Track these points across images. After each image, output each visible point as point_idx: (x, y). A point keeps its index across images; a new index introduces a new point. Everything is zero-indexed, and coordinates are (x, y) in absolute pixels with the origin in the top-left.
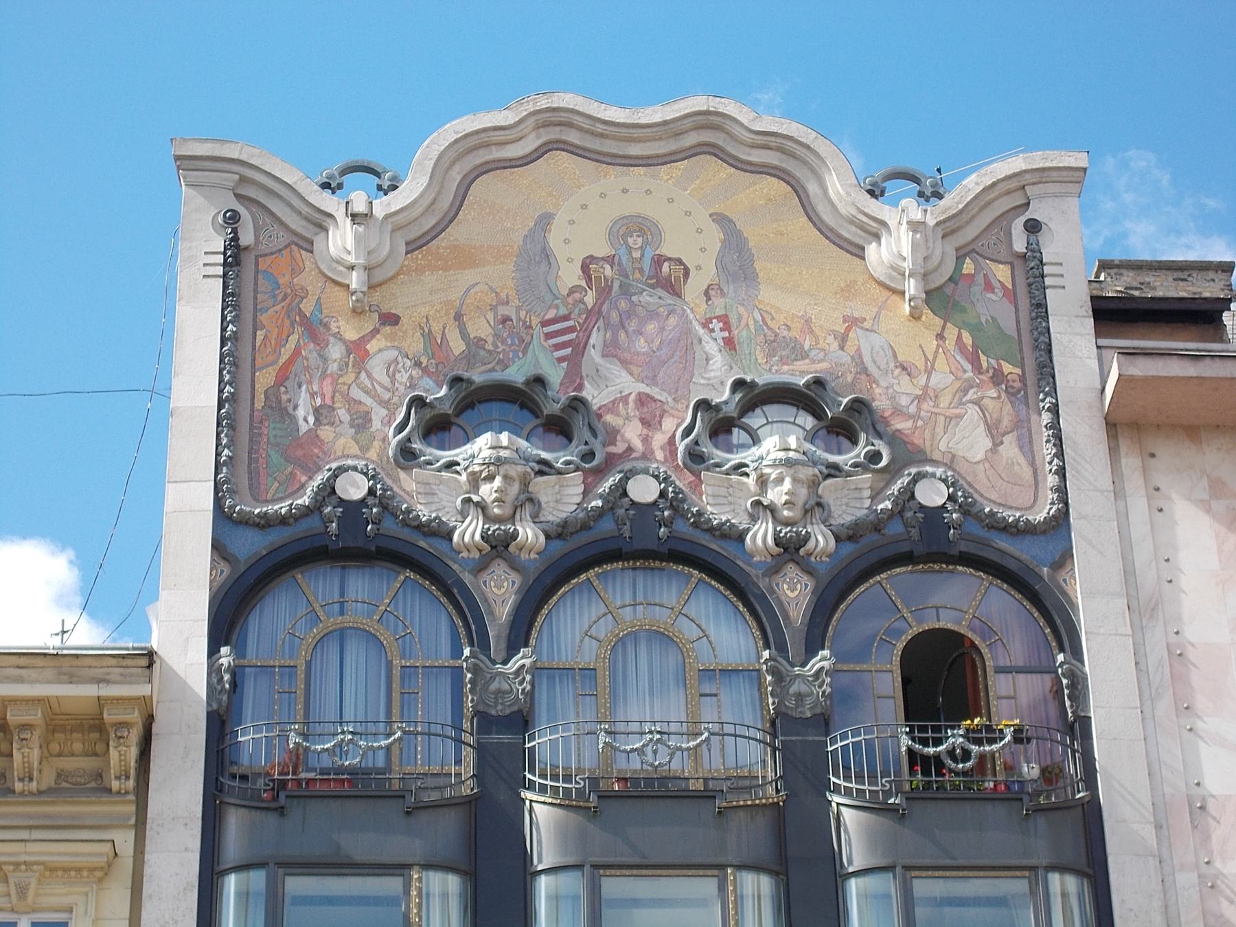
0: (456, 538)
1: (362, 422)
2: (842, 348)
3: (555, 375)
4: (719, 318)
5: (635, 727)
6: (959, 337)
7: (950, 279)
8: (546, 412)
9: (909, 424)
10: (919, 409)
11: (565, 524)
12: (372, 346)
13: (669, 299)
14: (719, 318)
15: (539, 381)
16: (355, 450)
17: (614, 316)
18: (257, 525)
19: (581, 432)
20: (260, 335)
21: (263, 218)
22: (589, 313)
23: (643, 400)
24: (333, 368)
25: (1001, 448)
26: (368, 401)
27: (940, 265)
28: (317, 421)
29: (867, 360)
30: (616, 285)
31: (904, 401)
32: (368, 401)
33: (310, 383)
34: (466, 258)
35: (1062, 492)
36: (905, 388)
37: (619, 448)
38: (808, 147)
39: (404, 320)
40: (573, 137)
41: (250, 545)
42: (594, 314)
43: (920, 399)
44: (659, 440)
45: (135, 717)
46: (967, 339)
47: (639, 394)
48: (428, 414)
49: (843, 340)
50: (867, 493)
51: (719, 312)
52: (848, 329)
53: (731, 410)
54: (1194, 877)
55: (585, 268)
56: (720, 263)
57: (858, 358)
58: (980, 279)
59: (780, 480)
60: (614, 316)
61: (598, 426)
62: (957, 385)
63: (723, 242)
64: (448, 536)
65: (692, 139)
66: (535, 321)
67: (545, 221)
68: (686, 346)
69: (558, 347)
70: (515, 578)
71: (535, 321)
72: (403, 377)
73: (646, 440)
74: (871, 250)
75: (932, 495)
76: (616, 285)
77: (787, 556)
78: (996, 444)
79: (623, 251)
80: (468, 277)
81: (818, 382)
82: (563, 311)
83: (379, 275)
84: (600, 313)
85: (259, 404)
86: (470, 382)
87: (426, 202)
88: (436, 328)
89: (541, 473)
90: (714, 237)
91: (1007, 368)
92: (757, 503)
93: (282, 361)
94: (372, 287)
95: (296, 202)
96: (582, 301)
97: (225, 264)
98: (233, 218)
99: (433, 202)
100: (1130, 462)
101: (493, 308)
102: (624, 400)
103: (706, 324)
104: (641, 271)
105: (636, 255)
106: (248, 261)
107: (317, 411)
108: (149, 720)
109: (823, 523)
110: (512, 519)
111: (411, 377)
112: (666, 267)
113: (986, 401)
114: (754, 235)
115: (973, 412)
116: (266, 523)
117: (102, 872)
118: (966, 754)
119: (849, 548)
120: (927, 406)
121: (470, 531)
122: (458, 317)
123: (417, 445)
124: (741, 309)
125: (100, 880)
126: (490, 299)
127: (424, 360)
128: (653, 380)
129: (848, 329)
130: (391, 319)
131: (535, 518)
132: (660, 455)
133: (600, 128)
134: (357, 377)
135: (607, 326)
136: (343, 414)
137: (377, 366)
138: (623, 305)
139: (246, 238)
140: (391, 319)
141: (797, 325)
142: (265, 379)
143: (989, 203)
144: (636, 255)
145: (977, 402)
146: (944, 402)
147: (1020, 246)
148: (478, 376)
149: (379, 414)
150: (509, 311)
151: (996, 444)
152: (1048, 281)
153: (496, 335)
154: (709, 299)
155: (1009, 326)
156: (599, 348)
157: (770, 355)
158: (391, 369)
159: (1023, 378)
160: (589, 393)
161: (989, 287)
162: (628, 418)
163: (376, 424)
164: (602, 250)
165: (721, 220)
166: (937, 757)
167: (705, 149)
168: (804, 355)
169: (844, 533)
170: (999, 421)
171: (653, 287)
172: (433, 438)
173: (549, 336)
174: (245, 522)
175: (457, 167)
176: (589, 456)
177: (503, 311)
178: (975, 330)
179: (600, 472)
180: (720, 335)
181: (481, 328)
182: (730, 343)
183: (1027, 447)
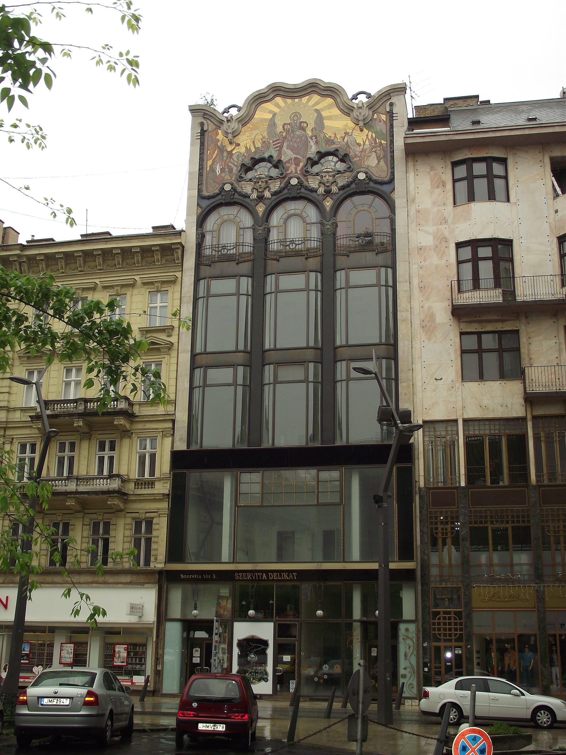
1: (231, 170)
2: (343, 141)
3: (275, 155)
4: (314, 136)
10: (361, 154)
11: (275, 192)
12: (234, 152)
13: (303, 132)
14: (314, 136)
18: (206, 199)
22: (284, 138)
23: (296, 158)
24: (225, 158)
26: (232, 165)
27: (367, 117)
29: (349, 143)
30: (290, 130)
31: (357, 153)
32: (232, 165)
33: (219, 163)
34: (256, 128)
37: (290, 171)
39: (241, 145)
41: (206, 203)
42: (285, 138)
43: (361, 152)
44: (299, 168)
47: (295, 158)
49: (344, 138)
50: (346, 178)
51: (315, 135)
52: (345, 136)
53: (316, 159)
54: (417, 266)
59: (325, 176)
60: (290, 138)
61: (285, 166)
62: (370, 148)
63: (317, 116)
64: (249, 197)
68: (306, 145)
69: (276, 147)
72: (241, 159)
73: (296, 169)
75: (361, 176)
76: (290, 130)
77: (327, 195)
78: (379, 162)
79: (292, 121)
80: (256, 132)
82: (278, 138)
85: (208, 169)
86: (255, 159)
89: (270, 180)
91: (383, 142)
92: (320, 183)
95: (216, 118)
100: (411, 164)
101: (262, 139)
103: (311, 138)
104: (297, 126)
106: (206, 134)
107: (221, 169)
108: (183, 247)
109: (336, 186)
111: (242, 159)
113: (378, 151)
114: (324, 114)
115: (374, 154)
116: (209, 198)
117: (174, 282)
119: (341, 192)
120: (363, 153)
122: (254, 142)
124: (320, 133)
127: (245, 154)
129: (345, 136)
130: (238, 145)
131: (269, 191)
132: (299, 172)
134: (230, 159)
136: (227, 170)
137: (235, 157)
139: (205, 129)
140: (238, 145)
141: (333, 135)
142: (210, 163)
144: (296, 122)
145: (375, 152)
148: (257, 157)
149: (235, 169)
151: (379, 162)
153: (262, 146)
154: (312, 131)
156: (286, 147)
158: (238, 157)
159: (386, 144)
160: (283, 159)
161: (380, 121)
162: (292, 164)
163: (234, 171)
167: (315, 92)
168: (333, 143)
170: (380, 156)
171: (299, 130)
173: (274, 145)
175: (254, 104)
176: (282, 174)
177: (264, 140)
179: (284, 178)
180: (314, 140)
181: (259, 145)
182: (317, 142)
183: (386, 162)
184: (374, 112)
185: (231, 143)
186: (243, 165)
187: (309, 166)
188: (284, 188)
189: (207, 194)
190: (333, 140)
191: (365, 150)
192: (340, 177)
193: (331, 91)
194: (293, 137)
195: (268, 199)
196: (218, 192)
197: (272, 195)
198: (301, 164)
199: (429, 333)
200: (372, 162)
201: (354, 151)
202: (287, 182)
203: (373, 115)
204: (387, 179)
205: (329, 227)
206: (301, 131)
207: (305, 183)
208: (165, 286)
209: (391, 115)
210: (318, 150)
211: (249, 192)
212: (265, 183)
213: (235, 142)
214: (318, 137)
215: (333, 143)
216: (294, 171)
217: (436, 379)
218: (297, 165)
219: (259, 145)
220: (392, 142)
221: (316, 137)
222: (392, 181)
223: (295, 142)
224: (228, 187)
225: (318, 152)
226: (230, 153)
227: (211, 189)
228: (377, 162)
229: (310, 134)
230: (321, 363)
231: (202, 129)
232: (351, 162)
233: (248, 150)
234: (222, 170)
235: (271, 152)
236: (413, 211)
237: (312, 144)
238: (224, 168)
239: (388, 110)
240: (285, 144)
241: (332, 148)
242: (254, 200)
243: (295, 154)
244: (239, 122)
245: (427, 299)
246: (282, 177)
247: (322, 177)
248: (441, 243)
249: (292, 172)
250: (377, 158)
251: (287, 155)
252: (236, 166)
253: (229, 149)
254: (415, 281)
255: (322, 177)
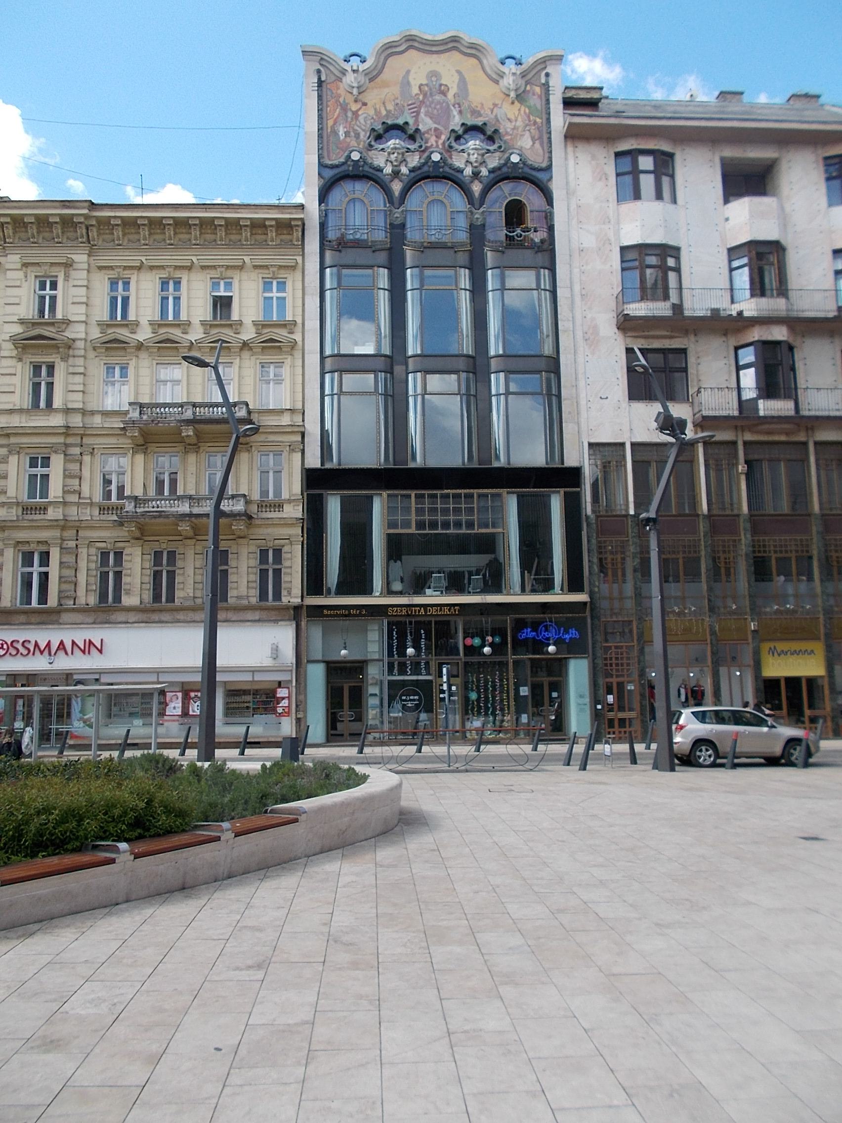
0: (384, 171)
1: (357, 136)
3: (411, 121)
5: (433, 228)
6: (525, 111)
7: (524, 91)
8: (409, 133)
9: (510, 137)
11: (414, 167)
12: (360, 113)
13: (443, 98)
15: (406, 123)
16: (356, 145)
17: (428, 103)
19: (418, 139)
20: (328, 109)
21: (328, 72)
22: (421, 102)
23: (436, 129)
24: (349, 119)
25: (535, 145)
26: (358, 129)
28: (345, 137)
29: (499, 116)
30: (428, 93)
31: (509, 130)
32: (358, 129)
34: (386, 85)
35: (550, 159)
36: (509, 126)
37: (429, 145)
38: (484, 48)
40: (416, 44)
41: (329, 174)
42: (422, 102)
44: (440, 142)
45: (300, 223)
46: (527, 111)
48: (375, 133)
51: (458, 102)
53: (460, 132)
54: (578, 270)
55: (420, 88)
56: (458, 87)
57: (496, 116)
58: (531, 92)
59: (473, 154)
60: (428, 103)
64: (382, 171)
65: (451, 45)
66: (406, 105)
67: (408, 72)
68: (448, 111)
70: (401, 184)
71: (406, 105)
72: (369, 122)
73: (437, 142)
74: (501, 81)
75: (515, 159)
76: (428, 93)
78: (534, 143)
80: (386, 90)
81: (485, 124)
82: (413, 101)
83: (361, 90)
84: (424, 103)
85: (329, 130)
87: (374, 66)
88: (378, 107)
89: (407, 152)
90: (456, 78)
91: (538, 120)
92: (467, 161)
93: (335, 117)
94: (359, 93)
95: (337, 66)
96: (418, 98)
97: (318, 86)
98: (319, 71)
99: (376, 66)
100: (570, 149)
101: (394, 101)
102: (431, 129)
103: (454, 106)
105: (434, 83)
106: (324, 84)
107: (345, 133)
108: (304, 225)
110: (399, 165)
112: (443, 88)
113: (532, 131)
116: (333, 167)
117: (293, 268)
118: (521, 235)
119: (492, 175)
120: (515, 131)
121: (388, 170)
122: (384, 103)
123: (373, 143)
125: (294, 270)
126: (393, 98)
127: (374, 117)
128: (439, 124)
130: (365, 104)
132: (440, 147)
133: (424, 41)
135: (426, 106)
136: (352, 134)
137: (361, 119)
138: (430, 99)
139: (323, 78)
140: (365, 104)
141: (479, 106)
143: (536, 66)
145: (529, 130)
146: (520, 129)
147: (543, 81)
148: (390, 122)
149: (362, 134)
150: (398, 101)
151: (534, 143)
152: (551, 92)
153: (395, 109)
155: (539, 107)
157: (472, 116)
159: (542, 123)
160: (420, 127)
161: (534, 94)
162: (432, 135)
164: (425, 82)
165: (458, 72)
166: (513, 236)
168: (480, 115)
169: (491, 170)
172: (378, 141)
173: (410, 109)
174: (326, 166)
176: (421, 147)
178: (529, 107)
179: (424, 151)
180: (458, 109)
181: (390, 107)
182: (460, 112)
183: (542, 144)
184: (527, 83)
185: (356, 101)
186: (373, 130)
187: (452, 140)
188: (424, 164)
189: (330, 163)
190: (479, 112)
191: (518, 128)
192: (489, 157)
193: (476, 49)
194: (432, 102)
195: (405, 175)
196: (343, 160)
197: (410, 171)
198: (443, 137)
199: (593, 347)
200: (526, 142)
201: (505, 127)
202: (428, 156)
203: (526, 86)
204: (544, 165)
205: (479, 216)
206: (441, 95)
207: (450, 161)
208: (282, 271)
209: (546, 87)
210: (462, 121)
211: (382, 165)
212: (401, 156)
213: (360, 101)
214: (461, 104)
215: (480, 115)
216: (434, 144)
217: (601, 398)
218: (438, 137)
219: (390, 107)
220: (548, 120)
221: (459, 104)
222: (549, 168)
223: (435, 108)
224: (355, 156)
225: (463, 124)
226: (356, 114)
227: (336, 158)
228: (531, 143)
229: (453, 101)
230: (474, 373)
231: (319, 79)
232: (501, 140)
233: (377, 112)
234: (347, 134)
235: (406, 118)
236: (573, 206)
237: (455, 112)
238: (349, 132)
239: (543, 81)
240: (423, 110)
241: (479, 122)
242: (388, 175)
243: (435, 123)
244: (366, 75)
245: (590, 308)
246: (422, 150)
247: (469, 154)
248: (604, 245)
249: (432, 145)
250: (532, 140)
251: (426, 124)
252: (364, 130)
253: (354, 108)
254: (577, 288)
255: (469, 154)
